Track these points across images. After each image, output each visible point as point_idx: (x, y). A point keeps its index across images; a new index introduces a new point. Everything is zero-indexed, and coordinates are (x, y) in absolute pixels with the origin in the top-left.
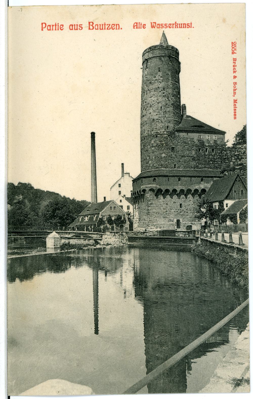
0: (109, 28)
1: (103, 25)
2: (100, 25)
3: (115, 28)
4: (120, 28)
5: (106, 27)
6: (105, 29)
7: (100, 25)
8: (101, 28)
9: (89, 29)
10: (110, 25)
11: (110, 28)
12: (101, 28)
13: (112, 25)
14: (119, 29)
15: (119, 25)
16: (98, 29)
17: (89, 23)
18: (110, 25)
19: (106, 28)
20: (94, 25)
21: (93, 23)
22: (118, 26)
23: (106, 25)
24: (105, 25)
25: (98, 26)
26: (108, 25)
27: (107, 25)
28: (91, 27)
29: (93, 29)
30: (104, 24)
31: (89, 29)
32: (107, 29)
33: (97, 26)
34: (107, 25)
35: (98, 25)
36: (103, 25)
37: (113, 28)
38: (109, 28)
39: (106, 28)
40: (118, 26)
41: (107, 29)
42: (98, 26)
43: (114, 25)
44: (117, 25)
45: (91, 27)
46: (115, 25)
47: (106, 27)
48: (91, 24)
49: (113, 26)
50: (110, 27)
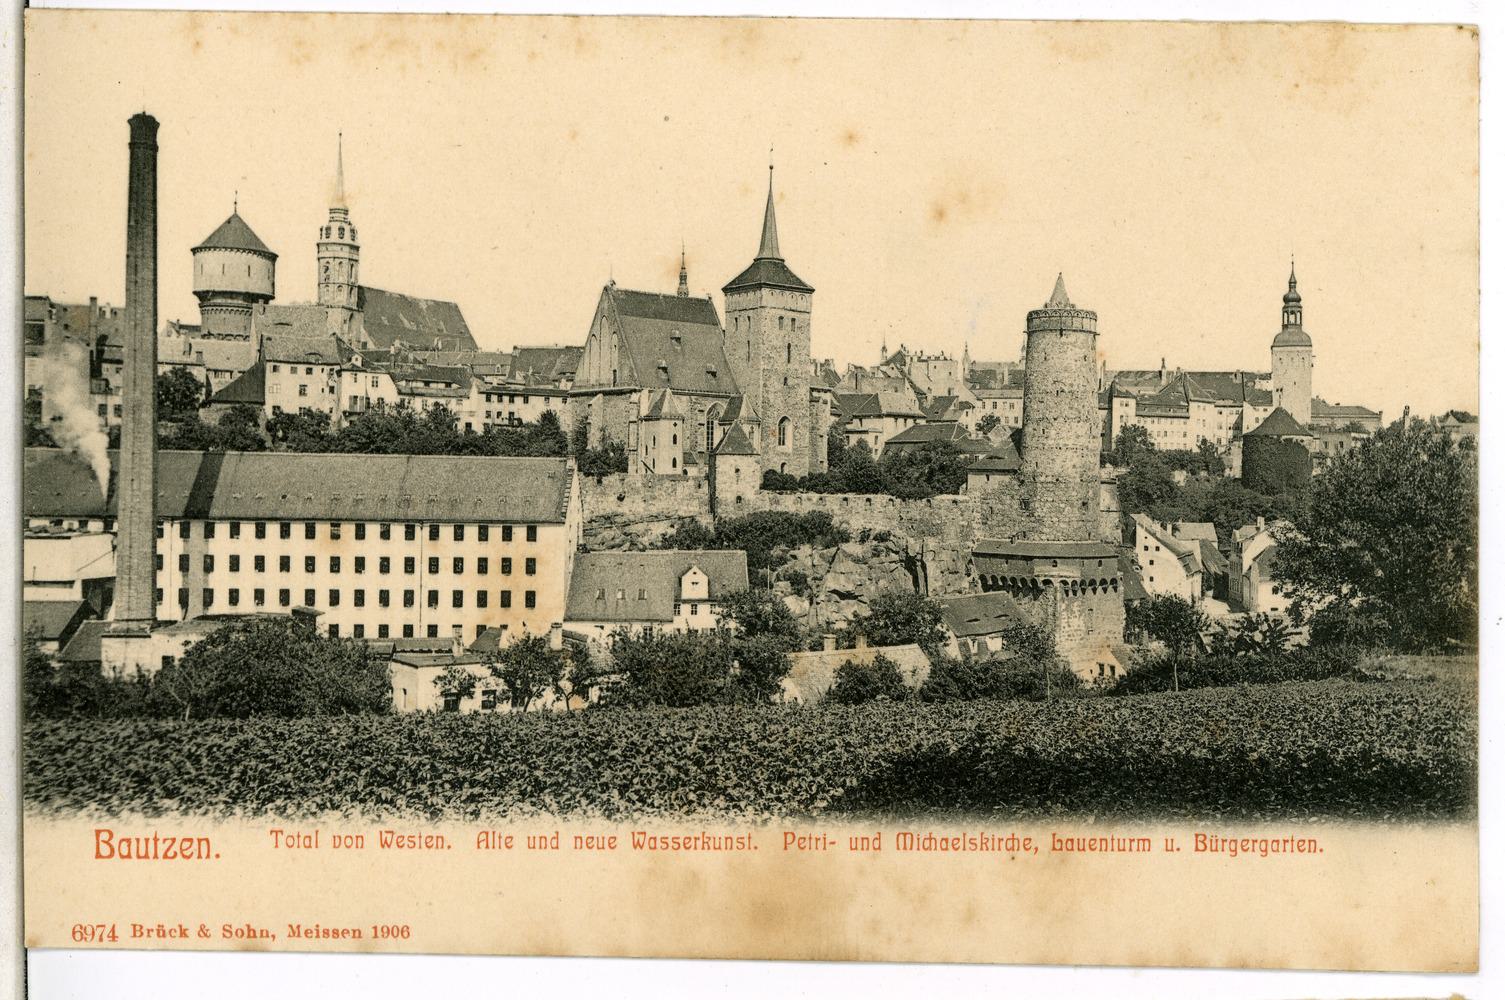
0: (170, 854)
1: (147, 840)
2: (138, 840)
4: (212, 854)
5: (162, 848)
6: (156, 856)
7: (138, 840)
8: (142, 853)
10: (174, 840)
11: (176, 853)
12: (142, 853)
14: (208, 856)
15: (207, 840)
16: (129, 856)
18: (174, 840)
19: (161, 854)
20: (115, 842)
21: (111, 835)
22: (204, 844)
24: (156, 840)
25: (129, 846)
26: (168, 843)
27: (165, 840)
30: (151, 837)
32: (165, 856)
33: (124, 844)
34: (165, 840)
35: (128, 841)
37: (187, 853)
38: (170, 854)
39: (161, 854)
40: (204, 844)
41: (165, 856)
42: (129, 846)
43: (191, 840)
44: (200, 841)
46: (196, 843)
47: (162, 848)
49: (186, 844)
50: (176, 847)
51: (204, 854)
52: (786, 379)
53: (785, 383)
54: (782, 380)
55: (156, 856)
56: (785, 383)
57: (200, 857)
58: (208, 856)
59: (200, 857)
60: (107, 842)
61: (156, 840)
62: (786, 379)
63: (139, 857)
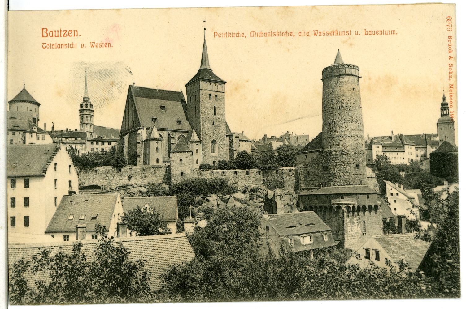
0: (65, 35)
1: (58, 31)
2: (55, 31)
3: (73, 35)
4: (78, 35)
5: (63, 33)
6: (61, 36)
7: (55, 31)
8: (57, 35)
9: (43, 36)
11: (67, 35)
12: (57, 35)
13: (70, 31)
14: (77, 36)
15: (77, 31)
17: (43, 29)
18: (66, 31)
19: (62, 35)
20: (48, 32)
21: (47, 30)
23: (62, 32)
25: (52, 33)
26: (65, 32)
27: (64, 31)
28: (45, 35)
29: (47, 36)
31: (43, 36)
32: (64, 36)
33: (51, 33)
35: (52, 31)
36: (58, 31)
38: (65, 35)
39: (62, 35)
40: (76, 32)
41: (64, 36)
42: (52, 33)
44: (74, 31)
45: (45, 35)
46: (73, 31)
47: (63, 33)
48: (45, 30)
49: (70, 32)
51: (76, 35)
52: (213, 123)
53: (213, 125)
54: (212, 123)
55: (61, 36)
56: (213, 125)
57: (74, 36)
58: (77, 36)
59: (74, 36)
60: (46, 32)
61: (61, 31)
62: (213, 123)
63: (55, 36)
